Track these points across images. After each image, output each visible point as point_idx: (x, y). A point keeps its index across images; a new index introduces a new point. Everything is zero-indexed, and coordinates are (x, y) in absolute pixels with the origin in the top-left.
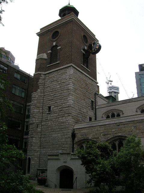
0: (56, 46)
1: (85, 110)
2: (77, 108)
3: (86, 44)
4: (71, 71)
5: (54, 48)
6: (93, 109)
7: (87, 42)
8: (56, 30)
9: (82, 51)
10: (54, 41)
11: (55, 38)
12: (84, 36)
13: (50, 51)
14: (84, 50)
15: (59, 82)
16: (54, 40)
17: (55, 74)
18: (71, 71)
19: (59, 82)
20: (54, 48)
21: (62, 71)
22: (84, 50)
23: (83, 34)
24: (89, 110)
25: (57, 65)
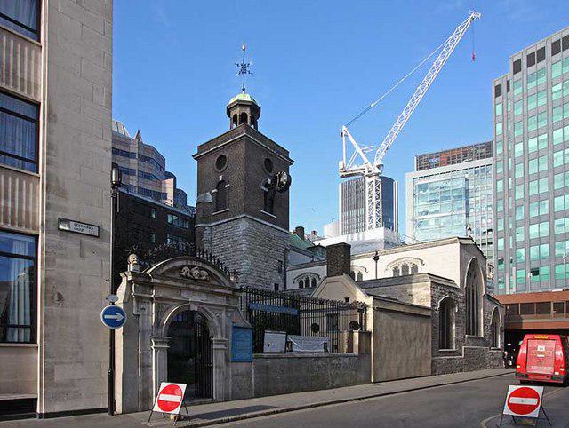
0: (223, 181)
1: (267, 276)
3: (271, 174)
4: (244, 225)
5: (220, 185)
6: (280, 272)
8: (221, 153)
9: (263, 188)
10: (220, 174)
14: (266, 185)
16: (220, 171)
17: (224, 227)
18: (244, 225)
20: (220, 185)
22: (266, 185)
23: (264, 157)
25: (226, 215)
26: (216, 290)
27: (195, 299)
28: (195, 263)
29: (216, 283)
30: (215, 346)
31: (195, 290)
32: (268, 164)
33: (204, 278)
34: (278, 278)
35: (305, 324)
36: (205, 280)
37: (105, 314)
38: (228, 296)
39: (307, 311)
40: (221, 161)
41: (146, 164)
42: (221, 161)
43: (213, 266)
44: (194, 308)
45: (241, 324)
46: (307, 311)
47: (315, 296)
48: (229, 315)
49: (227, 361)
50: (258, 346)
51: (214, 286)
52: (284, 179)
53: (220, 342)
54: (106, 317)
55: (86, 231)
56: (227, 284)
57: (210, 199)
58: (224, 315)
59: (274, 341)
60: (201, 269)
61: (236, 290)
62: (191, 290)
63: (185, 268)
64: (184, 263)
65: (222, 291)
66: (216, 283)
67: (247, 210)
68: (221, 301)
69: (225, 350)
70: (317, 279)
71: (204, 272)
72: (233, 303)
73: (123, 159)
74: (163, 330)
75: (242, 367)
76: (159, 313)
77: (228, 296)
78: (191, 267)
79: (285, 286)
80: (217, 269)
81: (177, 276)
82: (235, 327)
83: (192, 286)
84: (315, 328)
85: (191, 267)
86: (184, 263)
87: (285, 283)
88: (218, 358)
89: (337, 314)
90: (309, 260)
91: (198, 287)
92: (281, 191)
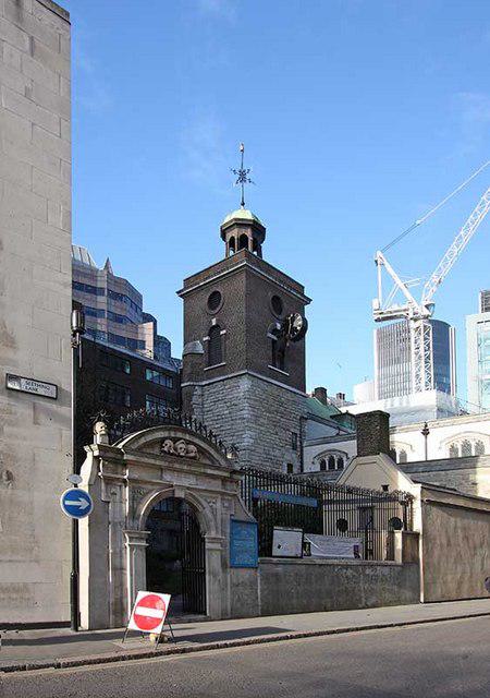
0: (217, 326)
1: (277, 453)
2: (262, 451)
4: (245, 384)
5: (213, 331)
6: (294, 448)
7: (280, 311)
9: (270, 335)
10: (214, 315)
11: (215, 308)
12: (276, 300)
13: (207, 338)
14: (274, 331)
15: (228, 404)
18: (245, 384)
19: (228, 404)
20: (213, 331)
21: (231, 382)
22: (274, 331)
24: (287, 450)
26: (209, 471)
27: (182, 483)
28: (179, 435)
29: (208, 462)
30: (208, 546)
31: (181, 471)
32: (276, 302)
33: (192, 455)
34: (292, 457)
35: (329, 518)
36: (194, 458)
37: (66, 498)
38: (224, 480)
39: (331, 502)
40: (215, 299)
41: (118, 304)
42: (215, 299)
43: (204, 440)
44: (180, 494)
45: (242, 517)
46: (331, 502)
47: (341, 482)
48: (226, 504)
49: (224, 565)
50: (265, 548)
51: (205, 465)
52: (298, 323)
53: (214, 540)
54: (67, 503)
55: (41, 391)
56: (223, 463)
57: (200, 349)
58: (219, 504)
59: (287, 541)
60: (189, 442)
61: (234, 472)
62: (175, 470)
63: (166, 442)
64: (166, 434)
65: (216, 472)
66: (208, 462)
67: (248, 365)
68: (216, 486)
69: (221, 551)
70: (345, 459)
71: (192, 447)
72: (231, 488)
73: (88, 296)
74: (140, 522)
75: (245, 574)
76: (135, 500)
77: (224, 480)
78: (175, 440)
79: (302, 467)
80: (210, 444)
81: (156, 451)
82: (233, 521)
83: (177, 466)
84: (342, 525)
85: (175, 440)
86: (166, 434)
87: (302, 463)
88: (213, 561)
89: (372, 508)
90: (334, 432)
91: (185, 467)
92: (295, 340)
